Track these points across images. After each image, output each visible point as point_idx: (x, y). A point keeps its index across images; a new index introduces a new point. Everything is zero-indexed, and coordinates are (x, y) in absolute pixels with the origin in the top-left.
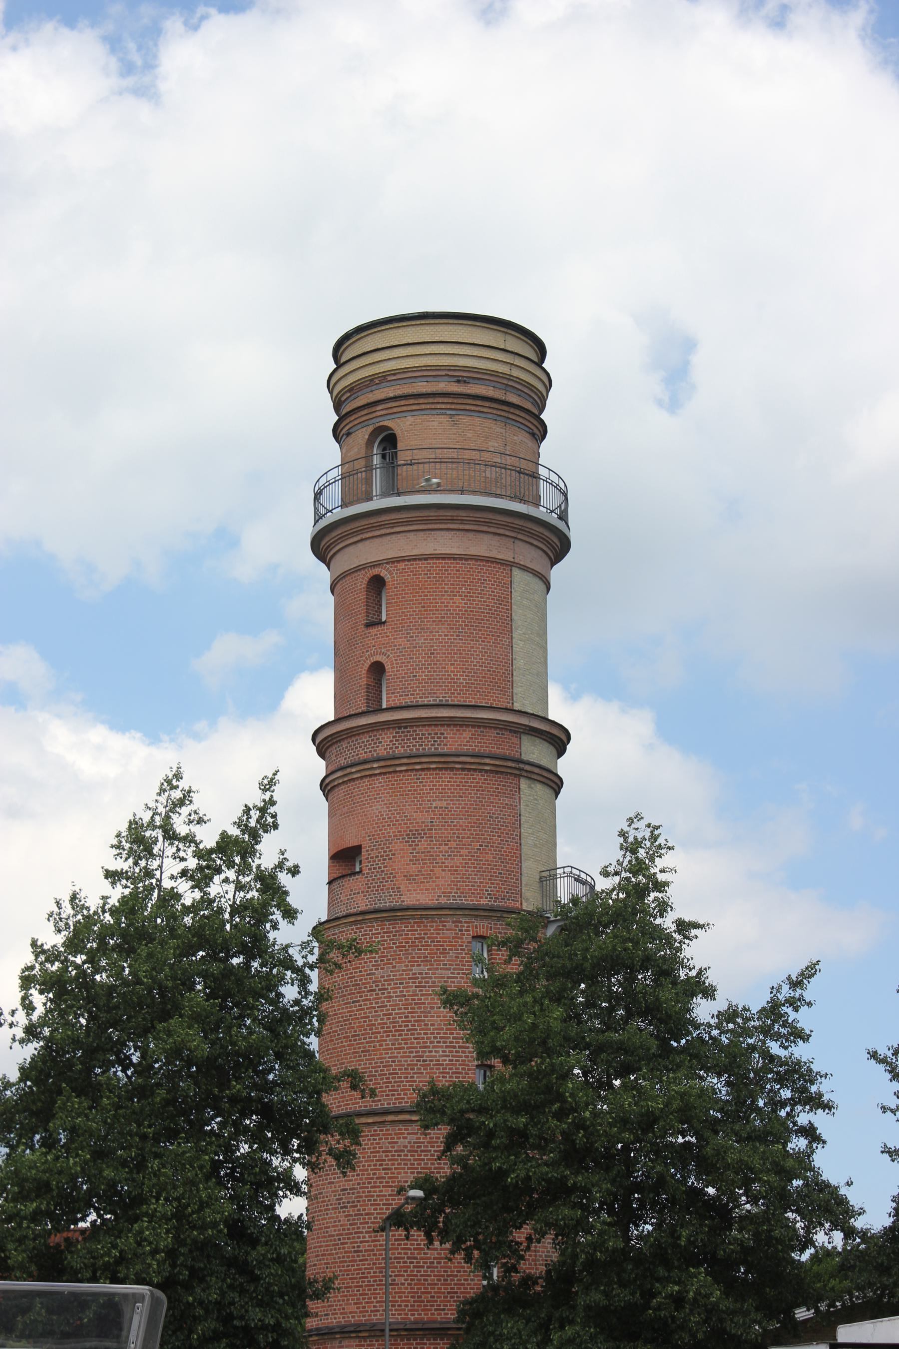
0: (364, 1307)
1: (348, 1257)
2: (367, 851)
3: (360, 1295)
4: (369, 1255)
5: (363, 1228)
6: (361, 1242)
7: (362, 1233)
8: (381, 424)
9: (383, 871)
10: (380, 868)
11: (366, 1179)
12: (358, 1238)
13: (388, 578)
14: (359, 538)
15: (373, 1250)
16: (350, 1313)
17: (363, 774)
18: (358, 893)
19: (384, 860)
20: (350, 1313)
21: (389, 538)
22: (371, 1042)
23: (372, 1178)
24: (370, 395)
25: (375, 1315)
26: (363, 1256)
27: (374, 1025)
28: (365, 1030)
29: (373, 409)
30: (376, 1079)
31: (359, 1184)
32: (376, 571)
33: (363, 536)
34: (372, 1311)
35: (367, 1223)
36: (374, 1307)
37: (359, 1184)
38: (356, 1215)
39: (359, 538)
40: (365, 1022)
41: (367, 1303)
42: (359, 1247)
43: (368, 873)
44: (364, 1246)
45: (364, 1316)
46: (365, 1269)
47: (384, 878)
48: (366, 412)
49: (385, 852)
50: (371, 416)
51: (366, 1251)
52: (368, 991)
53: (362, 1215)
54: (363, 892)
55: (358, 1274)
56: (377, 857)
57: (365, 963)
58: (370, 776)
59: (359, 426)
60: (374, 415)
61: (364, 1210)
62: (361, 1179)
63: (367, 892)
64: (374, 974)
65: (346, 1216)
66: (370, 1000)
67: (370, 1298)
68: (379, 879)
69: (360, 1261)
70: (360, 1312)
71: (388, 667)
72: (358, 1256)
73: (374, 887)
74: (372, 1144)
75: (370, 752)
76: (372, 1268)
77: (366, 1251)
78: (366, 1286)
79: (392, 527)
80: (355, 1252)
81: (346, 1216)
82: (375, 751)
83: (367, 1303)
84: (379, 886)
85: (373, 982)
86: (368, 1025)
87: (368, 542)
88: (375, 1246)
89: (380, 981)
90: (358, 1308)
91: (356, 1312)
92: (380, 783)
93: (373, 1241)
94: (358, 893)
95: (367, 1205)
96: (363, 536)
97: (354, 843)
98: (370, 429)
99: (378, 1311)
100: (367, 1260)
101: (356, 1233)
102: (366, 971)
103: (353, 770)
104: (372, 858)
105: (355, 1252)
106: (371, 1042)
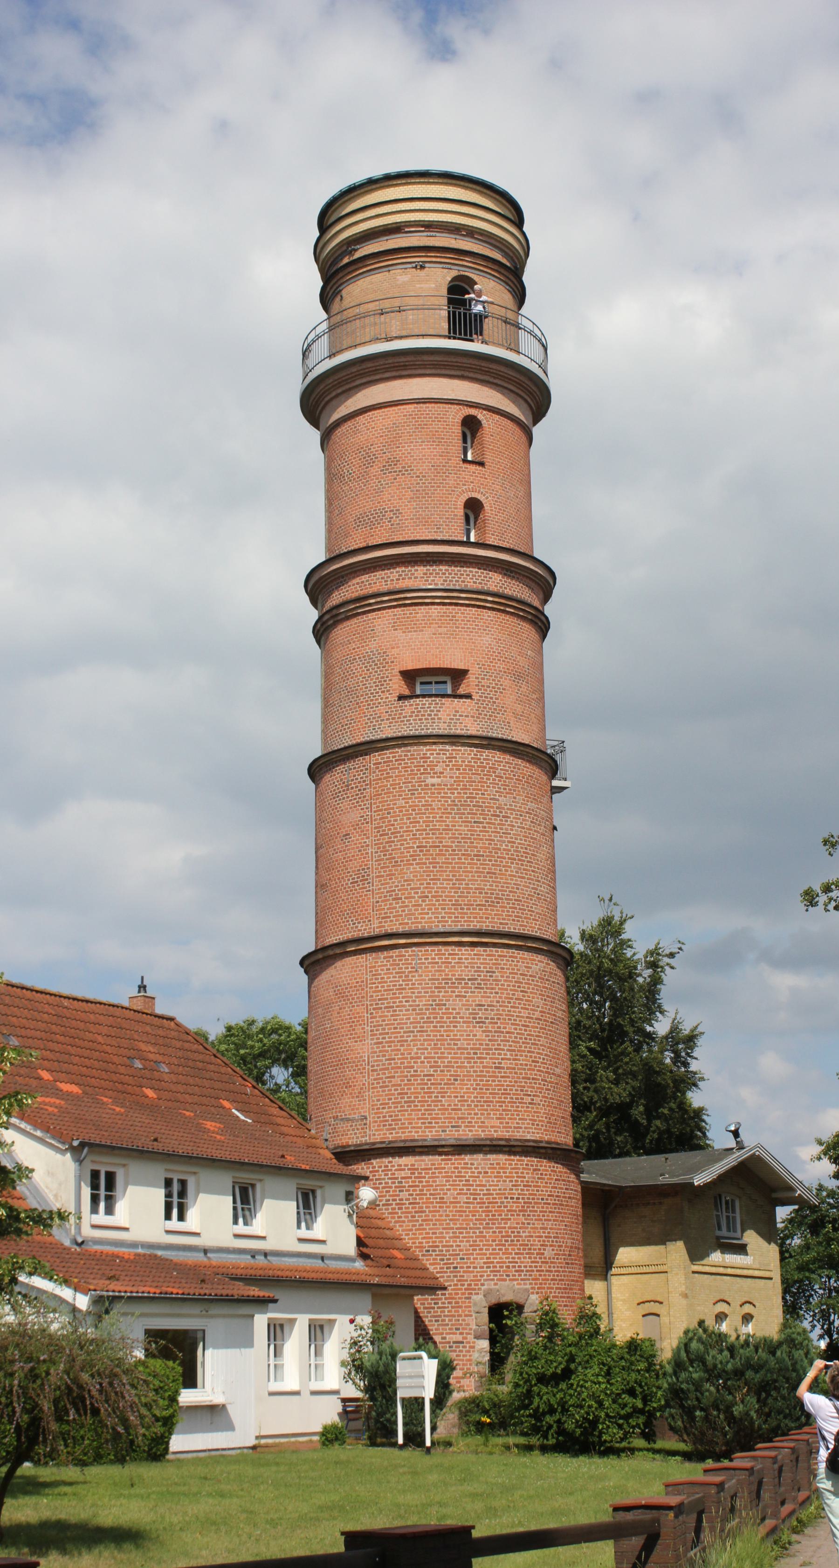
0: (508, 1123)
1: (487, 1072)
3: (504, 1110)
4: (511, 1073)
5: (505, 1045)
6: (502, 1059)
7: (503, 1050)
8: (466, 274)
9: (494, 702)
10: (491, 698)
11: (506, 998)
12: (500, 1054)
13: (484, 422)
15: (514, 1069)
16: (492, 1127)
17: (473, 603)
18: (466, 716)
19: (496, 692)
20: (492, 1127)
22: (497, 865)
23: (512, 999)
24: (453, 241)
25: (518, 1132)
26: (505, 1073)
27: (499, 849)
28: (491, 852)
30: (503, 903)
31: (498, 1002)
32: (473, 412)
33: (466, 374)
34: (515, 1128)
35: (508, 1041)
36: (518, 1123)
37: (498, 1002)
38: (495, 1032)
40: (490, 844)
41: (511, 1119)
42: (500, 1063)
43: (479, 700)
44: (506, 1063)
45: (508, 1132)
46: (508, 1086)
47: (495, 709)
49: (497, 684)
51: (508, 1068)
52: (492, 815)
53: (503, 1032)
55: (499, 1090)
56: (489, 687)
57: (488, 787)
58: (479, 607)
59: (441, 266)
61: (505, 1028)
62: (500, 997)
63: (478, 718)
64: (498, 800)
65: (484, 1032)
66: (494, 824)
67: (513, 1115)
68: (490, 709)
69: (502, 1077)
70: (504, 1127)
71: (487, 507)
72: (499, 1072)
73: (486, 715)
74: (511, 965)
75: (480, 583)
76: (514, 1086)
77: (508, 1068)
78: (509, 1102)
79: (495, 378)
80: (496, 1068)
81: (484, 1032)
82: (486, 584)
83: (511, 1119)
84: (491, 716)
85: (497, 808)
86: (493, 849)
88: (517, 1064)
89: (504, 809)
90: (501, 1123)
91: (499, 1127)
92: (489, 616)
93: (514, 1060)
94: (466, 716)
95: (508, 1024)
96: (466, 374)
97: (461, 666)
98: (454, 273)
99: (521, 1128)
100: (508, 1077)
101: (496, 1049)
102: (489, 795)
103: (490, 599)
104: (483, 686)
105: (496, 1068)
106: (497, 865)
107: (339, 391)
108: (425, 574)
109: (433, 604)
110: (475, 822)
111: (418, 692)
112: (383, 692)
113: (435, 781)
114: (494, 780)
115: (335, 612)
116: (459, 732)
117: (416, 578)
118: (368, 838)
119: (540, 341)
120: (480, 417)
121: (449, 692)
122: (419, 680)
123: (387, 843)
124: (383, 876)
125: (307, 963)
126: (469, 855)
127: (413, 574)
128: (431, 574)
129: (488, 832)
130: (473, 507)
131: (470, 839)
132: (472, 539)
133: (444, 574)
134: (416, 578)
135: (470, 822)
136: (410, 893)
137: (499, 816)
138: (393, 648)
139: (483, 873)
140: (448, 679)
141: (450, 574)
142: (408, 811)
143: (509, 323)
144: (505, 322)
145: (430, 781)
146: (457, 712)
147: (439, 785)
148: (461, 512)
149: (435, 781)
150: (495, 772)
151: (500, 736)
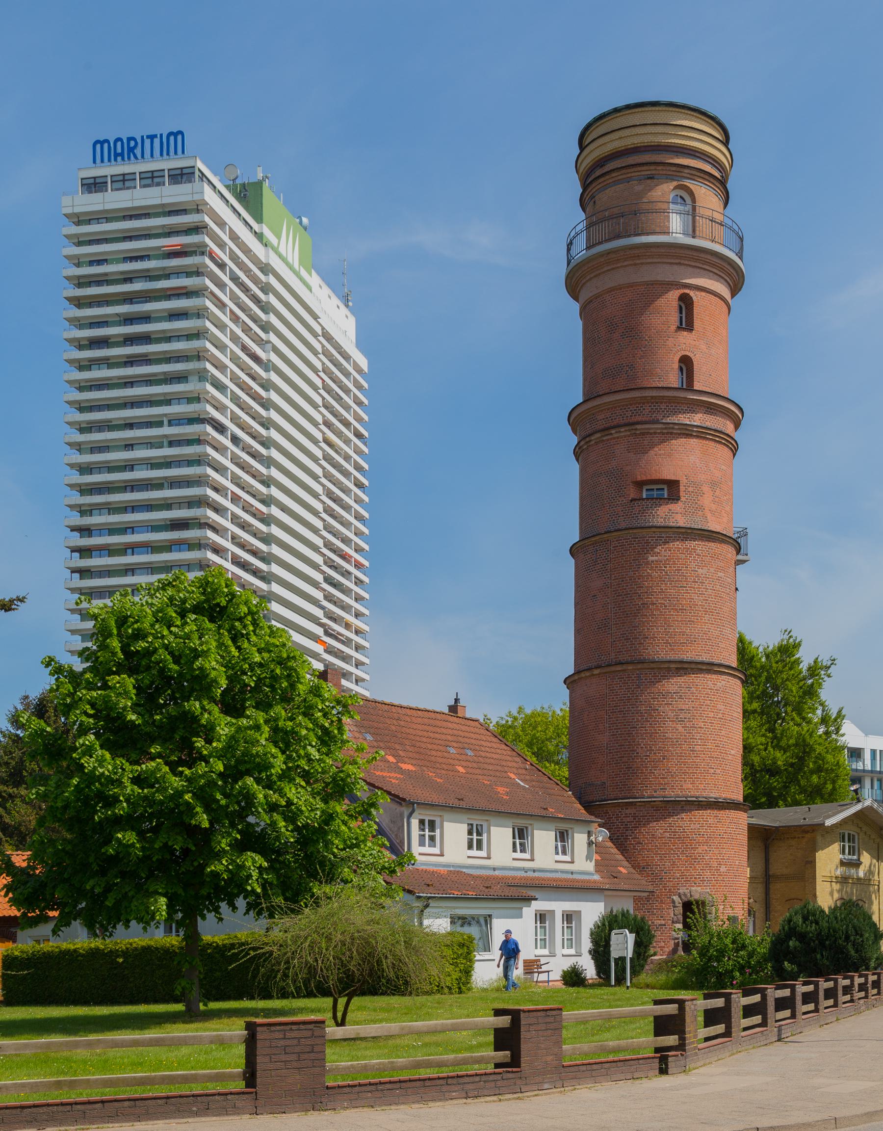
2: (684, 486)
10: (694, 500)
13: (694, 298)
14: (677, 261)
21: (698, 270)
29: (682, 170)
33: (682, 262)
39: (677, 261)
40: (690, 601)
48: (674, 169)
50: (678, 174)
52: (692, 582)
54: (681, 513)
60: (681, 174)
63: (685, 514)
84: (694, 513)
87: (683, 267)
94: (677, 513)
97: (673, 478)
107: (592, 275)
108: (650, 412)
109: (655, 433)
110: (681, 587)
111: (644, 497)
112: (620, 497)
113: (655, 558)
114: (694, 557)
115: (588, 439)
116: (671, 524)
117: (644, 415)
118: (608, 598)
119: (737, 234)
120: (692, 293)
121: (666, 496)
122: (645, 488)
123: (621, 601)
124: (618, 624)
125: (568, 682)
126: (676, 610)
127: (641, 412)
128: (654, 412)
129: (689, 593)
130: (686, 363)
131: (677, 598)
132: (685, 387)
133: (663, 411)
134: (644, 415)
135: (677, 587)
136: (636, 635)
137: (697, 582)
138: (627, 465)
139: (685, 621)
140: (665, 487)
141: (667, 411)
142: (635, 579)
143: (715, 222)
144: (712, 221)
145: (651, 558)
146: (670, 510)
147: (656, 561)
148: (676, 366)
149: (655, 558)
150: (695, 552)
151: (700, 527)
